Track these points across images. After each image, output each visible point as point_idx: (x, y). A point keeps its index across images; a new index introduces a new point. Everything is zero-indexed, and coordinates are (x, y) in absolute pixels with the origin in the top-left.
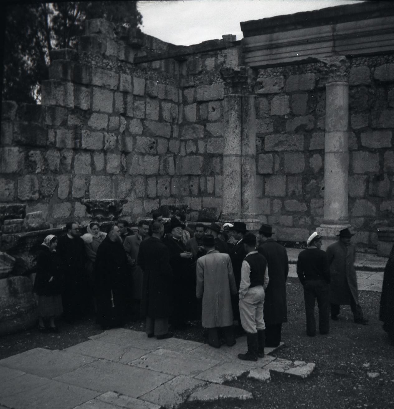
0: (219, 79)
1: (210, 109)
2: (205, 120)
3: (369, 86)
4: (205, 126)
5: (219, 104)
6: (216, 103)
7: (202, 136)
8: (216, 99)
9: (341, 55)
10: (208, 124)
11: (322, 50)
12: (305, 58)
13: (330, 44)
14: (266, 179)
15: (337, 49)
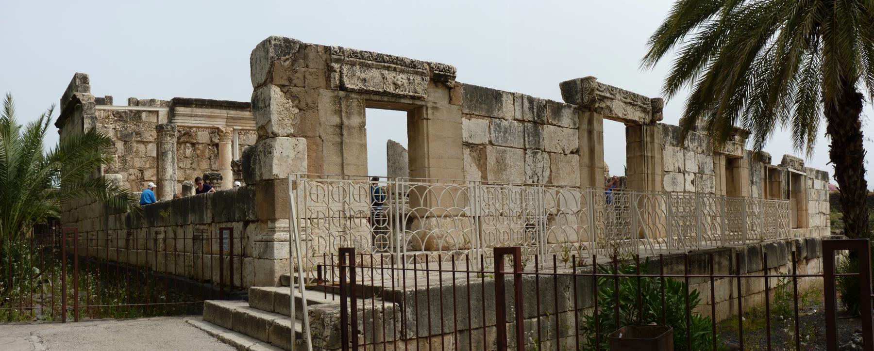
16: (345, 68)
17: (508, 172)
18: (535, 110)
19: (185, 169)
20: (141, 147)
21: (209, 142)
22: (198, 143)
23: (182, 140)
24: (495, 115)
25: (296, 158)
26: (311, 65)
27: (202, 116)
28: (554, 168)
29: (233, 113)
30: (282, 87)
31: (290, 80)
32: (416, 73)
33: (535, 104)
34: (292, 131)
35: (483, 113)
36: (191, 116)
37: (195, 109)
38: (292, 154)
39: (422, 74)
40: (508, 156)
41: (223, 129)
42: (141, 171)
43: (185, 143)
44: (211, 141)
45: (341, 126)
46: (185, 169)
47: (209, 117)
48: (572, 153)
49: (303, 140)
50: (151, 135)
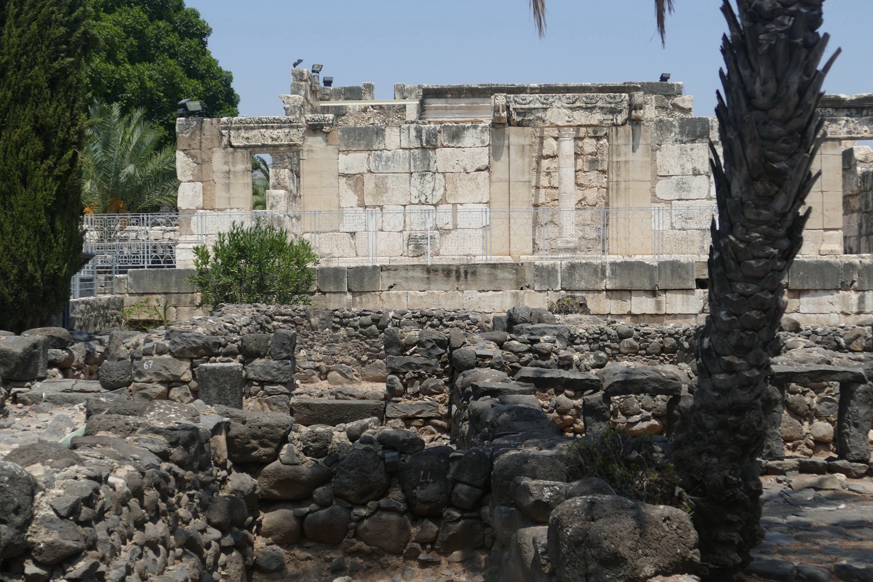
16: (232, 133)
17: (389, 194)
18: (424, 138)
24: (375, 147)
25: (194, 196)
26: (206, 133)
28: (449, 187)
30: (184, 150)
31: (189, 145)
32: (292, 127)
33: (424, 131)
34: (191, 178)
35: (362, 148)
38: (191, 194)
39: (298, 127)
40: (389, 181)
45: (229, 172)
48: (478, 170)
49: (199, 185)
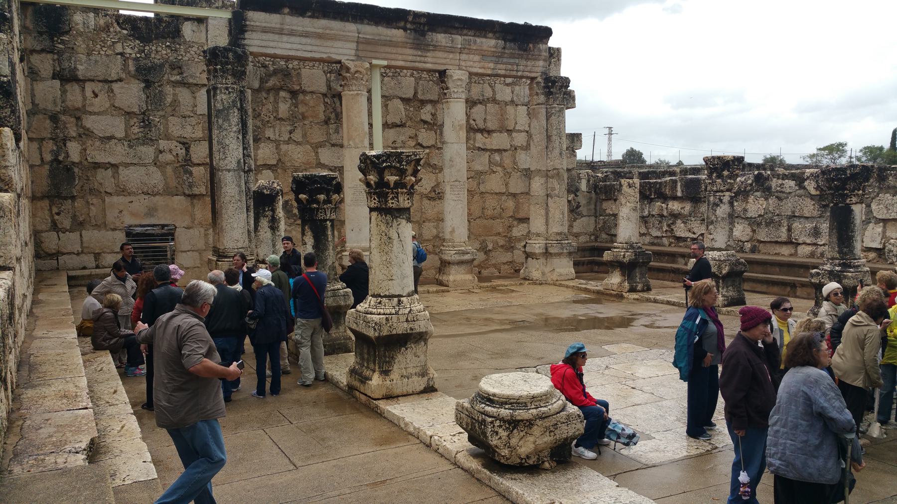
0: (104, 49)
1: (89, 94)
2: (78, 109)
3: (325, 95)
4: (78, 119)
5: (106, 87)
6: (101, 84)
7: (74, 134)
8: (101, 78)
9: (364, 61)
10: (84, 117)
11: (345, 51)
12: (324, 56)
13: (354, 45)
14: (195, 201)
15: (360, 54)
19: (277, 143)
20: (184, 95)
21: (324, 89)
22: (304, 92)
23: (270, 84)
27: (306, 35)
29: (370, 30)
36: (281, 32)
37: (288, 19)
41: (351, 65)
42: (186, 145)
43: (276, 90)
44: (329, 88)
46: (277, 143)
47: (320, 36)
50: (198, 72)
